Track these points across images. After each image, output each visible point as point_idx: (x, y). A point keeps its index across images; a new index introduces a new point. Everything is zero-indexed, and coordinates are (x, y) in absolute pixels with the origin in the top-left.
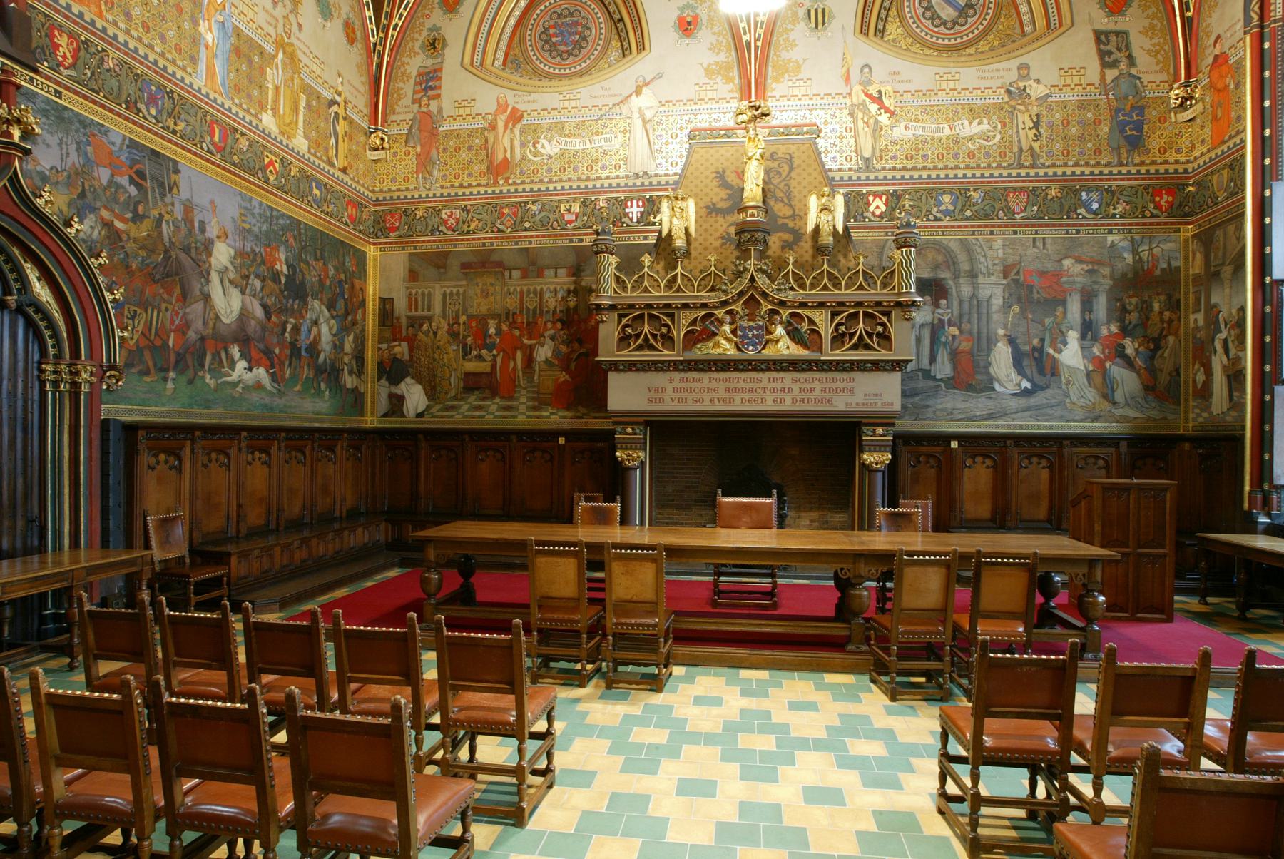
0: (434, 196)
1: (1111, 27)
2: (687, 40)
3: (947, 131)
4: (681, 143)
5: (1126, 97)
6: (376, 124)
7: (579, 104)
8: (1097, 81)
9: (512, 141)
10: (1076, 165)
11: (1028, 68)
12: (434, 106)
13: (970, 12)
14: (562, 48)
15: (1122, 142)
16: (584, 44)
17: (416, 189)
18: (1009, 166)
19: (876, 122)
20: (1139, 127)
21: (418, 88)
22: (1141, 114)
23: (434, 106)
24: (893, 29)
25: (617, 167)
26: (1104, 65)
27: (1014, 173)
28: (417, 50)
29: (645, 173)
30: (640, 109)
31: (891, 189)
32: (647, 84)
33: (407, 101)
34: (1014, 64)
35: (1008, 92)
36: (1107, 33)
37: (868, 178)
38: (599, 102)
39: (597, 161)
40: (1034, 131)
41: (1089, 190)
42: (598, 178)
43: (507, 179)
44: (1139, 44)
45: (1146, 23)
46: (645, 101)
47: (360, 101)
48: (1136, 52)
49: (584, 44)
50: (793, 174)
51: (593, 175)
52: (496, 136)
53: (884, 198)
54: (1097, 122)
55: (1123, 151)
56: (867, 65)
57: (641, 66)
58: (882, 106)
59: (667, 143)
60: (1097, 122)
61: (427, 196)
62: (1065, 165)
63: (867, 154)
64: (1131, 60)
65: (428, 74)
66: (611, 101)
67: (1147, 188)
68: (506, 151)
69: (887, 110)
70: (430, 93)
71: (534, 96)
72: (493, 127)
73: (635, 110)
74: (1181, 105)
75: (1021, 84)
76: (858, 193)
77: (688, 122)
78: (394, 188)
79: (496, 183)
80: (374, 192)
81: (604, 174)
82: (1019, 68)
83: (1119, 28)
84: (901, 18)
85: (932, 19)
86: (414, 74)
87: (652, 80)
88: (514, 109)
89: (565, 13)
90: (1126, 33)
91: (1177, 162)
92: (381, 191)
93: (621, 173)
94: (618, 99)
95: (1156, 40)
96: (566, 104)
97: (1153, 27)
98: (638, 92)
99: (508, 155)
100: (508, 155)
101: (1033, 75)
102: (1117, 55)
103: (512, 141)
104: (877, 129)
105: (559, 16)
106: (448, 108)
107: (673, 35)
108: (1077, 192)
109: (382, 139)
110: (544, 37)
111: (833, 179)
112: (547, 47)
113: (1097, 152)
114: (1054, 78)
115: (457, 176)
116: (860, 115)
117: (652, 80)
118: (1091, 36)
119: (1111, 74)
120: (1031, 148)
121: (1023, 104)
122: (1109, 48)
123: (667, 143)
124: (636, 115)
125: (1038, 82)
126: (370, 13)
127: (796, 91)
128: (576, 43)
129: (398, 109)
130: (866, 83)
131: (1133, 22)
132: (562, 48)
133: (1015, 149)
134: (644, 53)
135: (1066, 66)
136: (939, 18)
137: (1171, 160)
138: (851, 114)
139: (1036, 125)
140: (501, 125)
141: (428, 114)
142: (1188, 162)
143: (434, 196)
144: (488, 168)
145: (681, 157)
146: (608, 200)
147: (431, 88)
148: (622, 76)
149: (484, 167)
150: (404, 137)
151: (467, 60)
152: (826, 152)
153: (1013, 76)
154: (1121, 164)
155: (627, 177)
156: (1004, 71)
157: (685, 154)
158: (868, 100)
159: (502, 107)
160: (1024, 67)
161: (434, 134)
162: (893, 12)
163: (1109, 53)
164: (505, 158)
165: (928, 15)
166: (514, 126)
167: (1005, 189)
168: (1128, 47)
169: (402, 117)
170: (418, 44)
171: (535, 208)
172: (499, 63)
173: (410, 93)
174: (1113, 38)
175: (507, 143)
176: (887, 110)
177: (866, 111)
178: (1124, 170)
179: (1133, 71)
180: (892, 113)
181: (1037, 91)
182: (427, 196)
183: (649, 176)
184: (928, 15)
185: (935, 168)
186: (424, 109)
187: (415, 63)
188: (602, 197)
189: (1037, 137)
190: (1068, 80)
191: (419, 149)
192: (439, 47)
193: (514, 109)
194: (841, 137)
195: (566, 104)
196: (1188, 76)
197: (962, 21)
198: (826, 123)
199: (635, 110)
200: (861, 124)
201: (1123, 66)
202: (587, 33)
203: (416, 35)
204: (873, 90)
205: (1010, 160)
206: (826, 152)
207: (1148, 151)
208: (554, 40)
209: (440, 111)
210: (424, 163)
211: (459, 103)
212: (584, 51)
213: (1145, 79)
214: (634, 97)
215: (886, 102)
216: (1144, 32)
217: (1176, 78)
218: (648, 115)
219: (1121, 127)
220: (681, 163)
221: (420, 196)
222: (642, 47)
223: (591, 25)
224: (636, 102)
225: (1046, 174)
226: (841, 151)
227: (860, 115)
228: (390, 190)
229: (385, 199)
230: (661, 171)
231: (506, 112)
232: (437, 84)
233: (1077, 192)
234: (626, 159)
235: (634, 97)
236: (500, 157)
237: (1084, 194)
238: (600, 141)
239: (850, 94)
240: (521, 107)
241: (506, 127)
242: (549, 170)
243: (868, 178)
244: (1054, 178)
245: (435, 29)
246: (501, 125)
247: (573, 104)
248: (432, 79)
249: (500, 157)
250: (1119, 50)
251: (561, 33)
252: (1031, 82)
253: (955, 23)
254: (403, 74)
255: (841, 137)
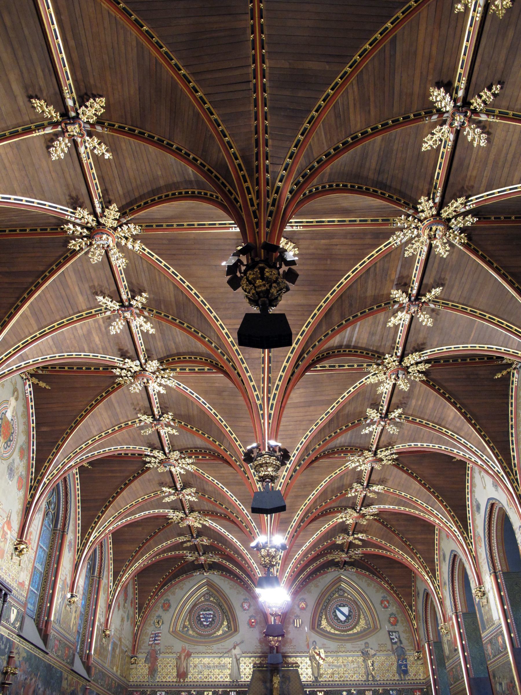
0: (155, 685)
1: (393, 630)
2: (252, 629)
3: (343, 666)
4: (250, 669)
5: (401, 655)
6: (134, 654)
7: (213, 651)
8: (390, 648)
9: (187, 664)
10: (387, 680)
11: (368, 644)
12: (157, 647)
13: (350, 618)
14: (205, 623)
15: (401, 672)
16: (213, 622)
17: (147, 682)
18: (365, 681)
19: (319, 663)
20: (406, 666)
21: (151, 639)
22: (406, 661)
23: (157, 647)
24: (324, 623)
25: (226, 677)
26: (393, 643)
27: (367, 683)
28: (152, 624)
29: (237, 680)
30: (235, 655)
31: (325, 689)
32: (238, 645)
33: (146, 644)
34: (363, 642)
35: (362, 652)
36: (392, 632)
37: (317, 685)
38: (220, 651)
39: (219, 675)
40: (372, 667)
41: (392, 690)
42: (219, 682)
43: (184, 680)
44: (403, 636)
45: (404, 628)
46: (237, 651)
47: (130, 647)
48: (402, 639)
49: (213, 622)
50: (290, 684)
51: (217, 680)
52: (181, 662)
53: (323, 693)
54: (392, 664)
55: (402, 675)
56: (314, 641)
57: (236, 638)
58: (320, 657)
59: (245, 669)
60: (392, 664)
61: (152, 685)
62: (384, 680)
63: (316, 675)
64: (400, 641)
65: (155, 634)
66: (225, 651)
67: (411, 689)
68: (184, 668)
69: (322, 659)
70: (156, 642)
71: (196, 647)
72: (179, 658)
73: (233, 655)
74: (418, 658)
75: (366, 650)
76: (314, 691)
77: (253, 661)
78: (138, 681)
79: (180, 681)
80: (130, 682)
81: (221, 680)
82: (365, 644)
83: (396, 630)
84: (326, 618)
85: (337, 620)
86: (150, 633)
87: (240, 643)
88: (188, 651)
89: (206, 609)
90: (398, 632)
91: (420, 679)
92: (133, 681)
93: (228, 680)
94: (227, 650)
95: (407, 635)
96: (208, 651)
97: (406, 630)
98: (235, 648)
99: (185, 670)
100: (185, 670)
101: (370, 646)
102: (396, 640)
103: (187, 664)
104: (319, 665)
105: (205, 611)
106: (162, 648)
107: (247, 627)
108: (389, 691)
109: (136, 660)
110: (198, 618)
111: (304, 685)
112: (199, 622)
113: (394, 675)
114: (376, 647)
115: (164, 677)
116: (313, 660)
117: (240, 643)
118: (387, 633)
119: (395, 647)
120: (372, 674)
121: (367, 657)
122: (393, 637)
123: (245, 669)
124: (234, 657)
125: (372, 649)
126: (137, 611)
127: (290, 650)
128: (210, 622)
129: (142, 647)
130: (315, 648)
131: (400, 627)
132: (205, 623)
133: (367, 674)
134: (236, 633)
135: (380, 643)
136: (339, 619)
137: (418, 678)
138: (310, 660)
139: (373, 665)
140: (183, 657)
141: (155, 651)
142: (423, 679)
143: (155, 685)
144: (177, 675)
145: (250, 674)
146: (223, 691)
147: (156, 640)
148: (229, 643)
149: (175, 674)
150: (144, 659)
151: (171, 630)
152: (302, 674)
153: (363, 647)
154: (402, 680)
155: (230, 682)
156: (361, 644)
157: (251, 673)
158: (315, 655)
159: (183, 650)
160: (366, 643)
161: (156, 659)
162: (324, 617)
163: (393, 639)
164: (184, 671)
165: (336, 618)
166: (188, 658)
167: (364, 690)
168: (399, 637)
169: (142, 651)
170: (152, 622)
171: (194, 693)
172: (181, 629)
173: (148, 640)
174: (394, 634)
175: (185, 665)
176: (322, 659)
177: (315, 659)
178: (403, 682)
179: (402, 646)
180: (324, 660)
181: (372, 652)
182: (152, 685)
183: (238, 682)
184: (336, 618)
185: (340, 681)
186: (153, 648)
187: (150, 630)
188: (220, 690)
189: (373, 669)
190: (381, 649)
191: (150, 665)
192: (160, 624)
193: (188, 651)
194: (307, 668)
195: (208, 651)
196: (419, 649)
197: (347, 621)
198: (301, 663)
199: (233, 655)
200: (314, 664)
201: (398, 644)
202: (215, 618)
203: (152, 618)
204: (317, 651)
205: (365, 678)
206: (302, 674)
207: (410, 675)
208: (202, 620)
209: (160, 650)
210: (153, 671)
211: (167, 647)
212: (213, 625)
213: (406, 648)
214: (233, 650)
215: (321, 654)
216: (403, 632)
217: (415, 649)
218: (238, 657)
219: (399, 666)
220: (250, 677)
221: (149, 685)
222: (236, 630)
223: (216, 615)
224: (234, 652)
225: (377, 684)
226: (307, 674)
227: (313, 660)
228: (136, 681)
229: (134, 685)
230: (243, 680)
231: (185, 652)
232: (159, 638)
233: (389, 691)
234: (230, 675)
235: (233, 650)
236: (182, 670)
237: (391, 692)
238: (220, 667)
239: (309, 652)
240: (191, 651)
241: (185, 658)
242: (201, 677)
243: (317, 685)
244: (380, 685)
245: (159, 616)
246: (183, 657)
247: (210, 651)
248: (157, 636)
249: (182, 670)
250: (396, 638)
251: (205, 618)
252: (369, 649)
253: (345, 621)
254: (146, 633)
255: (307, 668)
